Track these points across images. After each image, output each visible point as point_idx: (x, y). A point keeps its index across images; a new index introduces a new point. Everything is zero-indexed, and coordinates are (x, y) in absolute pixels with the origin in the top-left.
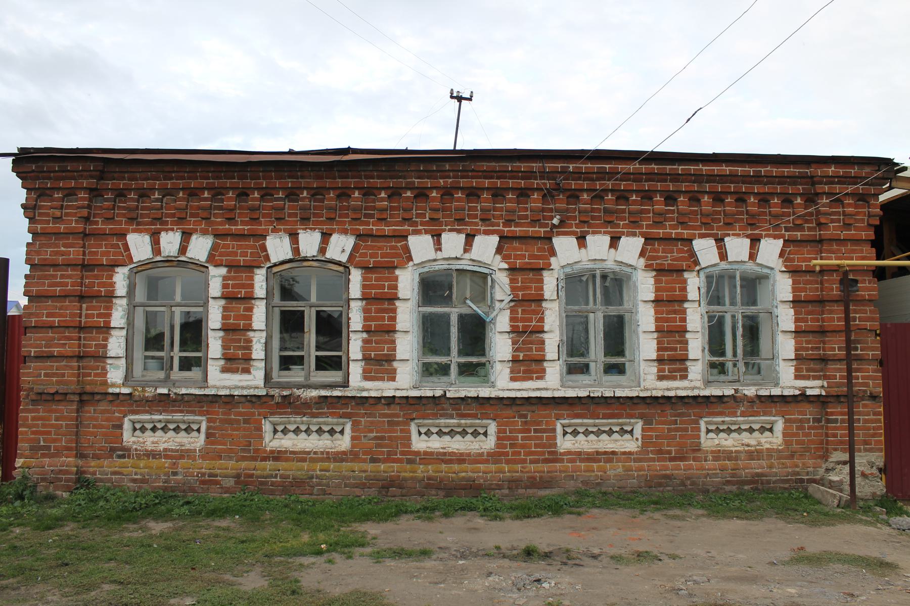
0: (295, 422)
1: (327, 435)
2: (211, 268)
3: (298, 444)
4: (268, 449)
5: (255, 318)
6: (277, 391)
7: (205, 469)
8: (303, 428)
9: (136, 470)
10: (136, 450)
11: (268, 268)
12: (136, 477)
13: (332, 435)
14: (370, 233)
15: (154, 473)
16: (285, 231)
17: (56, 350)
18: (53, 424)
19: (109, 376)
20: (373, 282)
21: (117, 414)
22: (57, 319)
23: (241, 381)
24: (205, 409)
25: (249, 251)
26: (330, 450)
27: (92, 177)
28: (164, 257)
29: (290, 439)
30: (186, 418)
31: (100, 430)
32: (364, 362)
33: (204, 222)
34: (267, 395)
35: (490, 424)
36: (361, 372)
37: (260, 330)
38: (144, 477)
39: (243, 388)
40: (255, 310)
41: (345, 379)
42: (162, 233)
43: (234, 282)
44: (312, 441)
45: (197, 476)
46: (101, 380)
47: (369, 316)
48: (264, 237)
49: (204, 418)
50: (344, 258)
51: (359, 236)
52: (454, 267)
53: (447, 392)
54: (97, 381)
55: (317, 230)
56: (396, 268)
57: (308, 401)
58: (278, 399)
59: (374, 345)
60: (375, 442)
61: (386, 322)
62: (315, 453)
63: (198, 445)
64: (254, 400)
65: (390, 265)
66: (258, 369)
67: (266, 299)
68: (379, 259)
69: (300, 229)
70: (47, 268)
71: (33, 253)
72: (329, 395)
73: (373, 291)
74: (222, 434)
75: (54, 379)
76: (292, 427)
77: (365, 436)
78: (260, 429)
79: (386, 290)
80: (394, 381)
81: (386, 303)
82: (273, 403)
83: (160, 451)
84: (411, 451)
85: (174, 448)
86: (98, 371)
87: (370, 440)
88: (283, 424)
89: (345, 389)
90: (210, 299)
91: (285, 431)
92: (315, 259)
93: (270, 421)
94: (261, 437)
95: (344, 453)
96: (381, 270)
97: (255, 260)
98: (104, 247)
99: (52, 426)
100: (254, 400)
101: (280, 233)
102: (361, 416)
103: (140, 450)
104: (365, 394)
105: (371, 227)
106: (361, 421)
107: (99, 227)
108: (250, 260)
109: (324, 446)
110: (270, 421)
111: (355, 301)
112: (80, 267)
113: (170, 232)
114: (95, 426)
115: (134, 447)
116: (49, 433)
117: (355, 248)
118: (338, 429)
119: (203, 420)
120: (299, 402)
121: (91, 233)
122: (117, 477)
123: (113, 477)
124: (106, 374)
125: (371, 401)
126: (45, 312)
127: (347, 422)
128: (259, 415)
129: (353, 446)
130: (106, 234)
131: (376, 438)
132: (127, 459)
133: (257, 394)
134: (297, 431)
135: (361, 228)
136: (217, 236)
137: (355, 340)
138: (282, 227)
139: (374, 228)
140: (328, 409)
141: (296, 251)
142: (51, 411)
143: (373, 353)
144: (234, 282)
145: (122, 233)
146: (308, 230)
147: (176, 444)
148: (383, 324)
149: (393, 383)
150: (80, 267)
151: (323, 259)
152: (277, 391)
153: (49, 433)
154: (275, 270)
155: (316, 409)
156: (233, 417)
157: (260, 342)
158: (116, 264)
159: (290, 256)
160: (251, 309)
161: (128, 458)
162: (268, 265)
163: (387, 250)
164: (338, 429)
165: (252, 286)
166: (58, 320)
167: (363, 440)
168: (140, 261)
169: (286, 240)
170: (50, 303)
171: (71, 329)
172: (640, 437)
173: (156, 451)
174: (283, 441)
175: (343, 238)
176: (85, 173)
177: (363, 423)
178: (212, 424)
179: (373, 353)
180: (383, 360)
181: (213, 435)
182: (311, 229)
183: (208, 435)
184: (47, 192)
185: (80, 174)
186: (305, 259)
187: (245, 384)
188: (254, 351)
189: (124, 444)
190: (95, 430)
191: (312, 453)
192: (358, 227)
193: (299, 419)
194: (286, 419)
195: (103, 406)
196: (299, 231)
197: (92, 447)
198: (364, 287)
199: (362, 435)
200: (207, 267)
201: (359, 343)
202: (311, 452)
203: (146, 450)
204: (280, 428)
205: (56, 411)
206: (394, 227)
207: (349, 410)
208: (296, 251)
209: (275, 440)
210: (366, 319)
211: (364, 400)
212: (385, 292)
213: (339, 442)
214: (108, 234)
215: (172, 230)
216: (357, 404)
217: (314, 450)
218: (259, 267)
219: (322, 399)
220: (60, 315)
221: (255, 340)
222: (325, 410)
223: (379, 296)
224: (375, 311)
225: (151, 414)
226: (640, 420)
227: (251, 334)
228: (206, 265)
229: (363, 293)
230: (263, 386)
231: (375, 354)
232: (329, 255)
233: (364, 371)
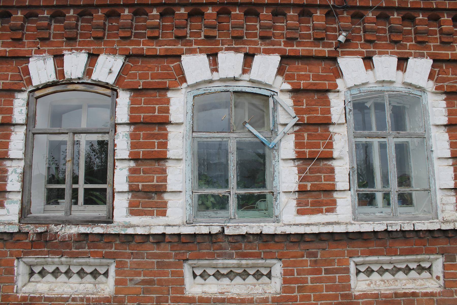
0: (53, 263)
1: (89, 278)
3: (56, 289)
4: (20, 295)
5: (12, 146)
6: (32, 227)
8: (63, 269)
11: (31, 92)
13: (95, 278)
14: (140, 52)
16: (49, 52)
20: (143, 105)
25: (10, 73)
26: (91, 296)
29: (47, 282)
32: (130, 194)
34: (19, 232)
35: (275, 264)
36: (127, 205)
37: (18, 159)
40: (13, 137)
41: (110, 214)
44: (72, 285)
47: (137, 143)
48: (26, 59)
50: (111, 80)
51: (128, 57)
52: (231, 89)
53: (225, 229)
55: (83, 51)
56: (167, 89)
57: (67, 239)
58: (32, 237)
59: (142, 174)
60: (142, 287)
61: (156, 149)
64: (5, 237)
65: (161, 86)
66: (13, 202)
67: (26, 125)
68: (150, 80)
69: (66, 50)
72: (89, 232)
73: (142, 115)
76: (50, 269)
77: (131, 280)
78: (11, 272)
79: (156, 114)
80: (165, 216)
81: (157, 128)
82: (27, 241)
84: (184, 297)
87: (136, 284)
88: (41, 265)
89: (109, 225)
91: (42, 273)
92: (80, 81)
93: (24, 262)
94: (12, 282)
96: (152, 92)
97: (15, 83)
100: (5, 237)
101: (44, 55)
102: (127, 256)
104: (130, 231)
105: (141, 46)
106: (127, 262)
108: (10, 84)
109: (85, 292)
110: (24, 262)
111: (122, 126)
117: (124, 70)
118: (102, 270)
120: (57, 240)
125: (138, 239)
127: (112, 263)
128: (11, 255)
129: (117, 291)
131: (144, 282)
133: (8, 231)
134: (56, 273)
135: (131, 47)
137: (121, 169)
138: (46, 48)
139: (145, 47)
140: (89, 248)
141: (60, 72)
143: (140, 184)
146: (74, 51)
148: (152, 152)
149: (164, 218)
151: (89, 81)
152: (32, 227)
154: (38, 94)
155: (76, 249)
157: (16, 172)
159: (53, 78)
160: (8, 136)
162: (31, 88)
163: (158, 70)
164: (102, 270)
165: (11, 111)
167: (129, 285)
169: (50, 62)
172: (441, 275)
174: (39, 285)
175: (111, 58)
177: (129, 264)
179: (140, 184)
180: (152, 192)
182: (77, 50)
186: (70, 82)
188: (9, 181)
191: (70, 300)
192: (127, 47)
193: (56, 260)
194: (43, 260)
196: (64, 52)
198: (132, 110)
199: (128, 278)
201: (126, 173)
202: (69, 298)
204: (37, 269)
206: (166, 47)
207: (113, 250)
208: (60, 72)
209: (30, 284)
210: (133, 146)
211: (130, 238)
212: (155, 116)
213: (102, 286)
216: (123, 243)
217: (73, 296)
218: (20, 91)
219: (82, 238)
221: (10, 170)
222: (86, 250)
223: (148, 120)
224: (143, 136)
226: (441, 256)
227: (8, 163)
229: (131, 117)
230: (17, 221)
231: (143, 185)
232: (95, 77)
233: (131, 205)
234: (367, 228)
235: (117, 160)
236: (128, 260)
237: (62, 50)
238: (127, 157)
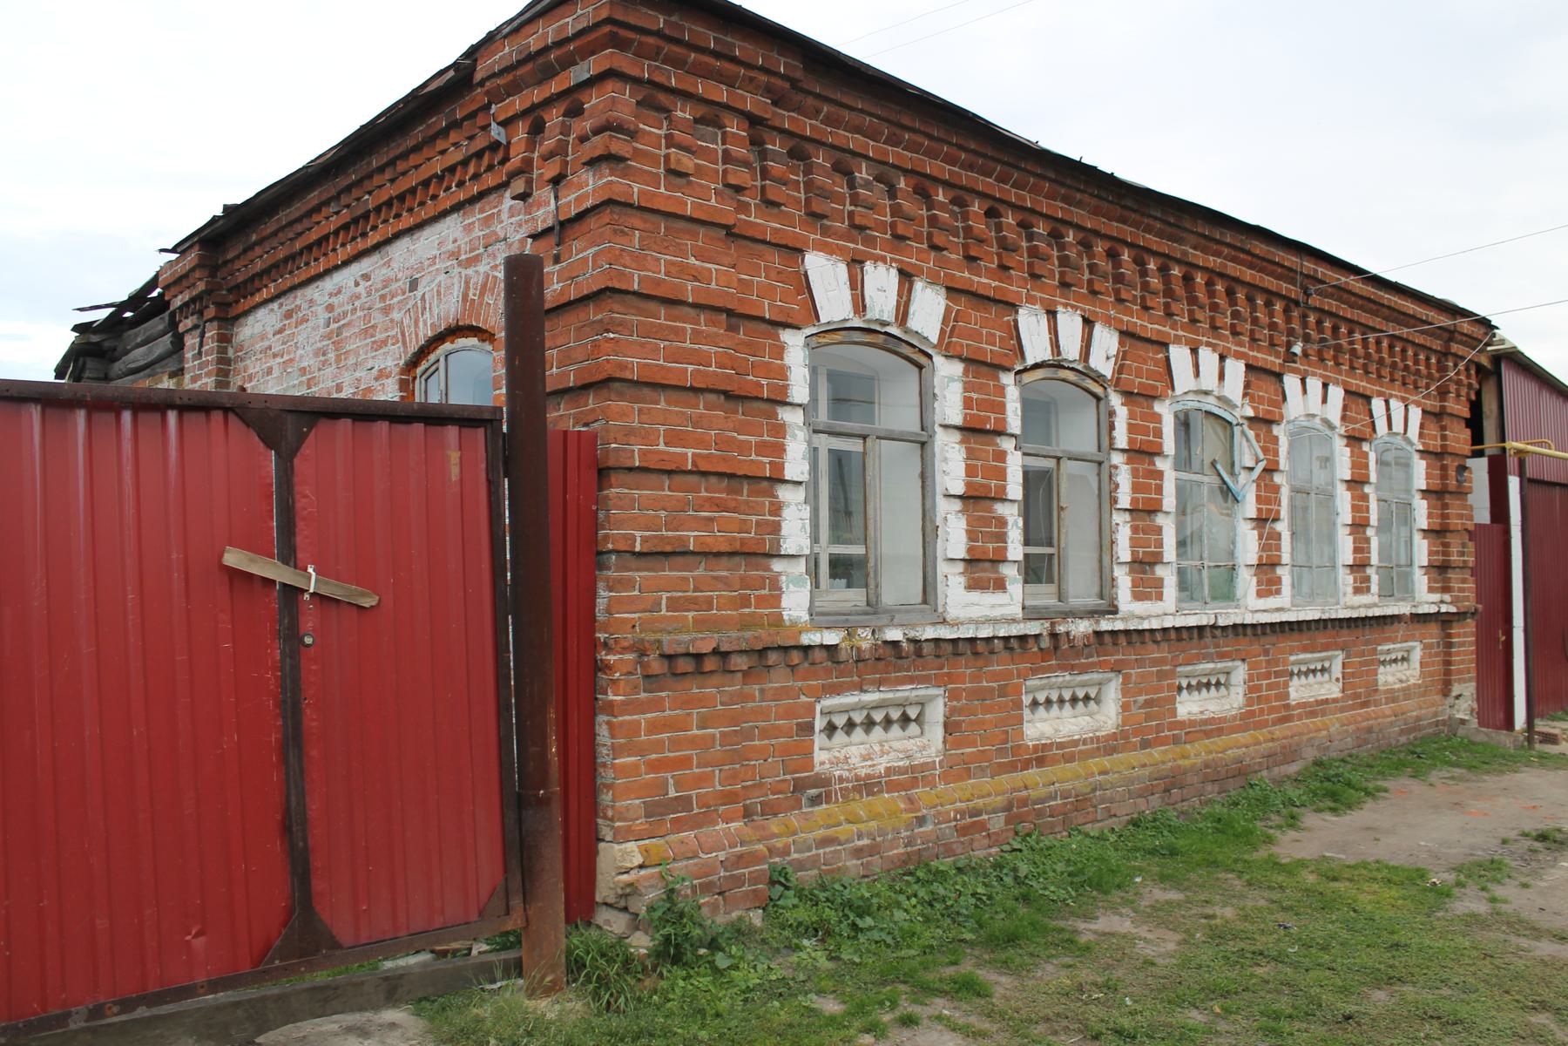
2: (938, 360)
7: (961, 802)
9: (858, 826)
10: (841, 779)
12: (860, 843)
15: (890, 828)
17: (692, 537)
18: (697, 735)
19: (785, 603)
21: (803, 699)
22: (690, 452)
23: (993, 606)
24: (946, 670)
27: (768, 90)
30: (915, 693)
31: (773, 741)
33: (933, 254)
35: (1238, 667)
36: (1130, 585)
38: (874, 839)
39: (995, 621)
42: (868, 263)
43: (981, 396)
45: (955, 820)
46: (770, 613)
49: (940, 691)
52: (1204, 409)
53: (1219, 617)
54: (761, 616)
56: (1154, 398)
62: (1085, 742)
63: (933, 751)
70: (652, 306)
71: (627, 260)
74: (971, 722)
75: (691, 614)
80: (1161, 600)
83: (880, 776)
84: (1176, 722)
85: (901, 764)
86: (763, 592)
90: (938, 429)
95: (1114, 736)
99: (693, 742)
103: (848, 780)
104: (1146, 625)
106: (1131, 674)
114: (765, 734)
115: (837, 773)
116: (685, 762)
119: (937, 696)
122: (828, 850)
123: (821, 851)
124: (779, 597)
126: (662, 428)
130: (764, 242)
132: (824, 806)
136: (950, 290)
142: (688, 703)
144: (981, 396)
146: (1069, 309)
147: (901, 756)
149: (1159, 603)
153: (685, 762)
156: (985, 684)
158: (790, 321)
161: (827, 803)
162: (1018, 367)
166: (694, 455)
170: (662, 405)
171: (713, 480)
172: (1340, 676)
173: (873, 777)
176: (764, 78)
178: (955, 703)
181: (958, 725)
183: (949, 727)
184: (663, 98)
185: (752, 74)
187: (997, 613)
188: (1009, 541)
189: (817, 769)
190: (766, 742)
195: (779, 680)
197: (761, 785)
200: (930, 357)
203: (858, 778)
205: (701, 701)
215: (884, 260)
220: (701, 443)
225: (863, 691)
226: (1340, 652)
228: (930, 351)
234: (1192, 621)
235: (1116, 509)
236: (1132, 671)
237: (1056, 303)
238: (1128, 507)
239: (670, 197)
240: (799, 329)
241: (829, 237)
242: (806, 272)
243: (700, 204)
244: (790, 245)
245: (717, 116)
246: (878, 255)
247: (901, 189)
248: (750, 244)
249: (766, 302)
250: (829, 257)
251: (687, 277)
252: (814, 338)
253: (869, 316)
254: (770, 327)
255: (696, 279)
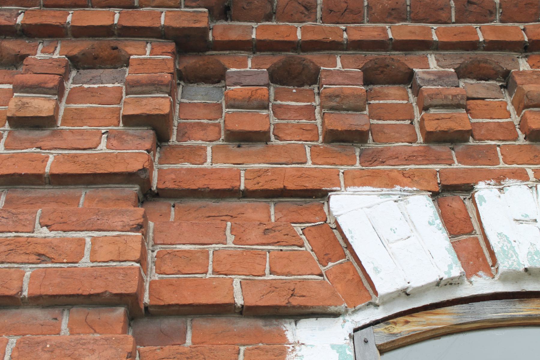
28: (506, 278)
42: (481, 185)
98: (230, 238)
107: (207, 165)
112: (121, 311)
113: (508, 182)
121: (170, 185)
145: (309, 185)
150: (121, 311)
158: (296, 302)
168: (406, 293)
214: (247, 194)
215: (522, 176)
239: (12, 156)
240: (336, 315)
241: (383, 163)
242: (336, 222)
243: (76, 156)
244: (291, 186)
245: (115, 48)
246: (502, 170)
247: (523, 73)
248: (211, 203)
249: (237, 281)
250: (385, 190)
251: (24, 258)
252: (380, 329)
253: (504, 265)
254: (260, 323)
255: (42, 257)
